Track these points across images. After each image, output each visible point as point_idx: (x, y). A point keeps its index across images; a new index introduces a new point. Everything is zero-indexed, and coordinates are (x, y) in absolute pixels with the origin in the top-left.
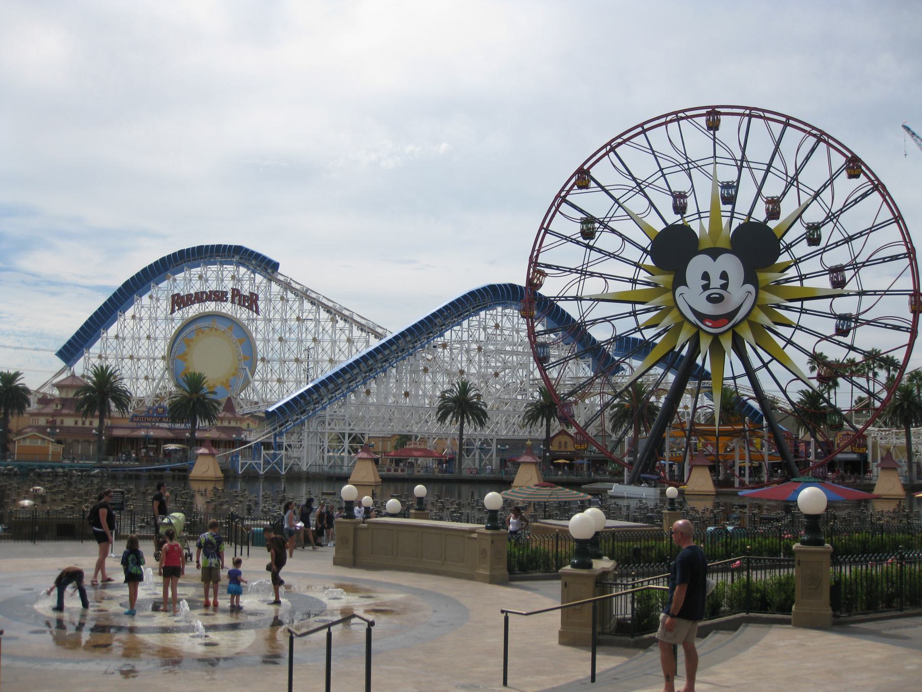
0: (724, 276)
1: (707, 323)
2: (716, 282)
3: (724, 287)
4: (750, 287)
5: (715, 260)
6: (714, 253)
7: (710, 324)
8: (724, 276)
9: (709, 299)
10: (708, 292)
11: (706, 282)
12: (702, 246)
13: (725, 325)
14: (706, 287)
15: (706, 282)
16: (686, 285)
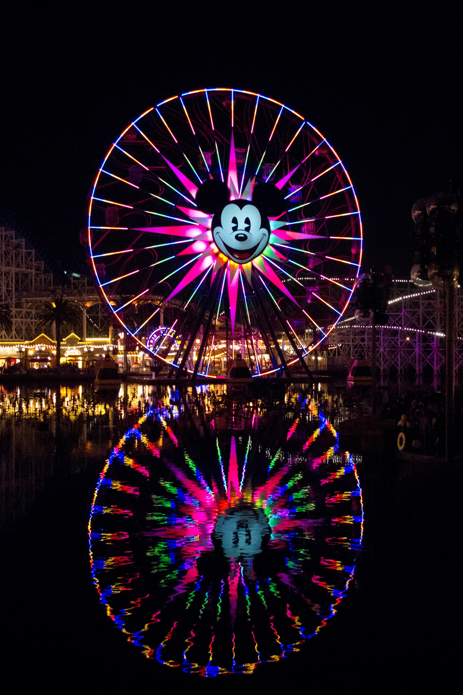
0: (247, 221)
1: (235, 256)
2: (242, 225)
3: (248, 229)
4: (264, 231)
5: (241, 208)
6: (241, 204)
7: (238, 257)
8: (247, 221)
9: (237, 238)
10: (236, 233)
11: (235, 225)
12: (233, 198)
13: (249, 257)
14: (235, 229)
15: (235, 225)
16: (221, 226)
